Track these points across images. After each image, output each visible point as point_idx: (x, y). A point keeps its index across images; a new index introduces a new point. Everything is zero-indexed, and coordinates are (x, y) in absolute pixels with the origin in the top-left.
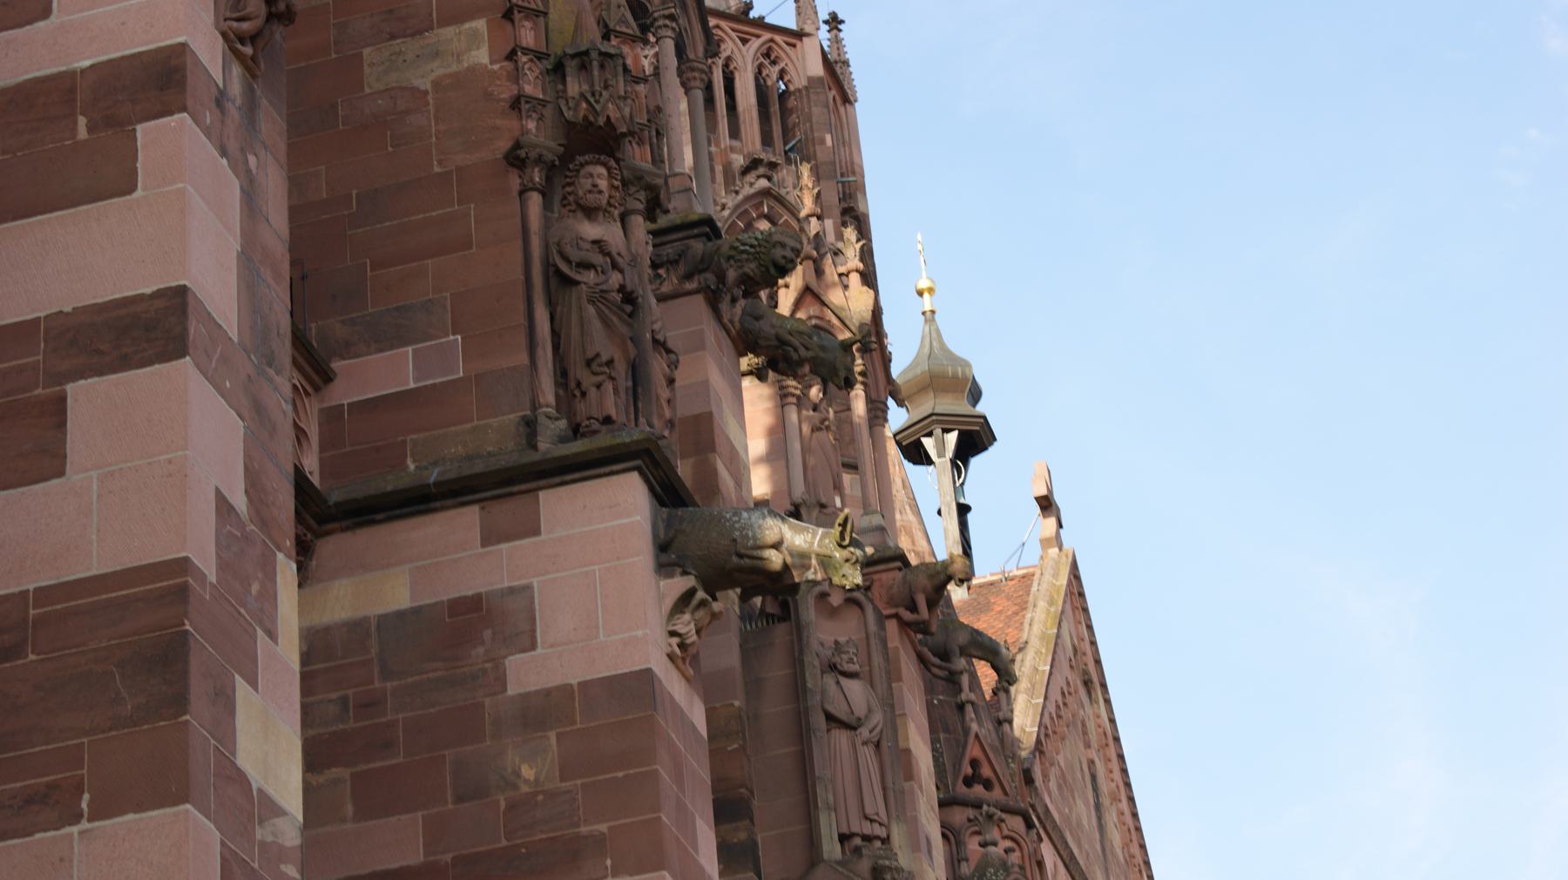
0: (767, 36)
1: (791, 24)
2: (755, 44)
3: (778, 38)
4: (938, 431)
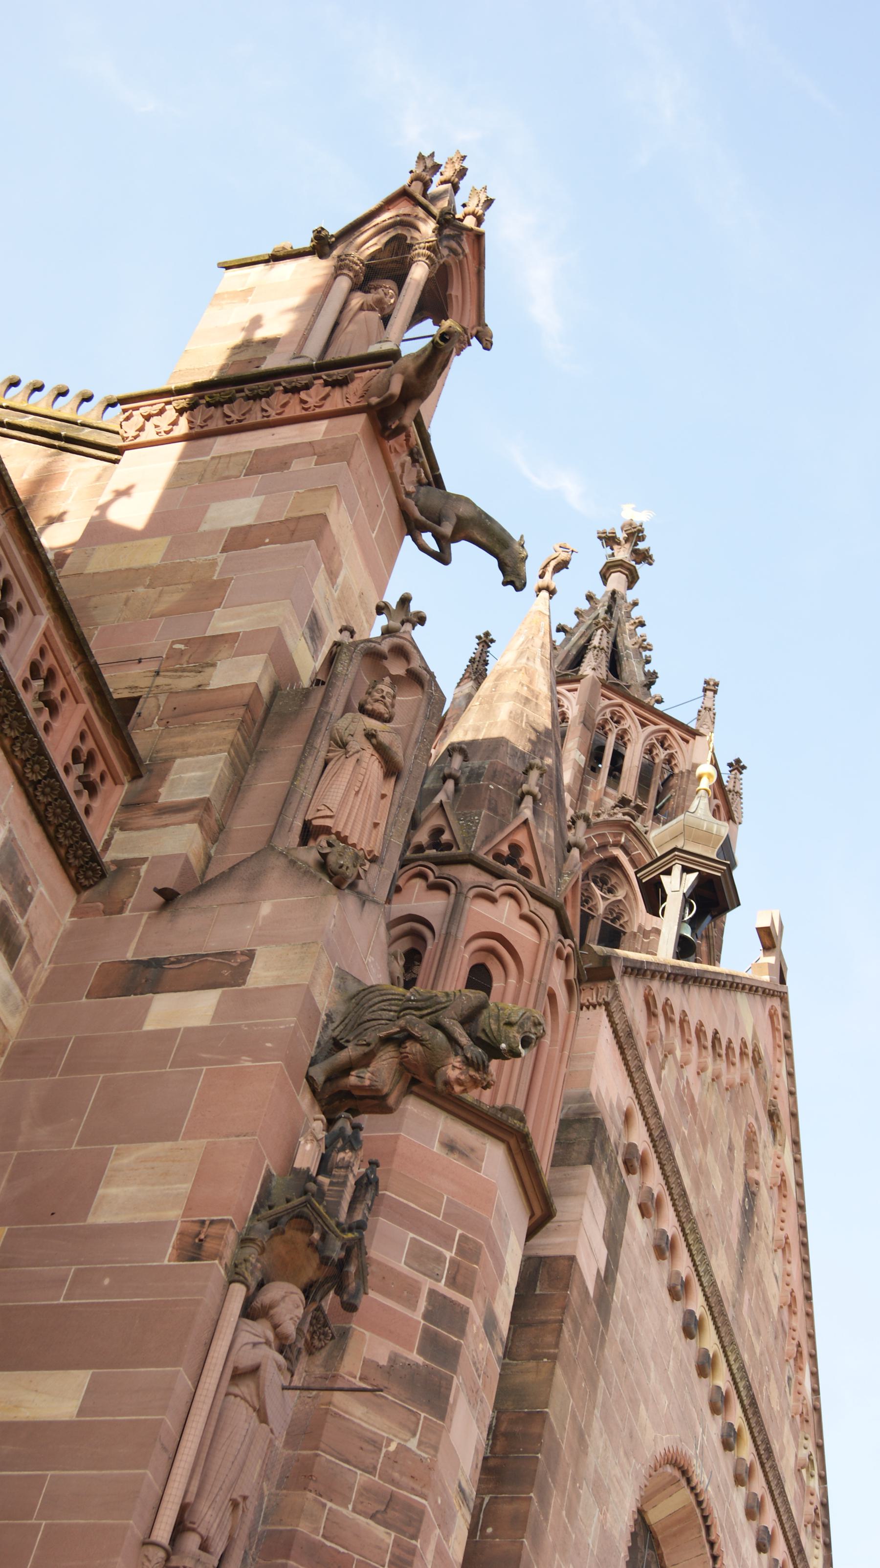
0: (664, 726)
1: (687, 716)
2: (652, 728)
3: (674, 731)
4: (677, 870)
